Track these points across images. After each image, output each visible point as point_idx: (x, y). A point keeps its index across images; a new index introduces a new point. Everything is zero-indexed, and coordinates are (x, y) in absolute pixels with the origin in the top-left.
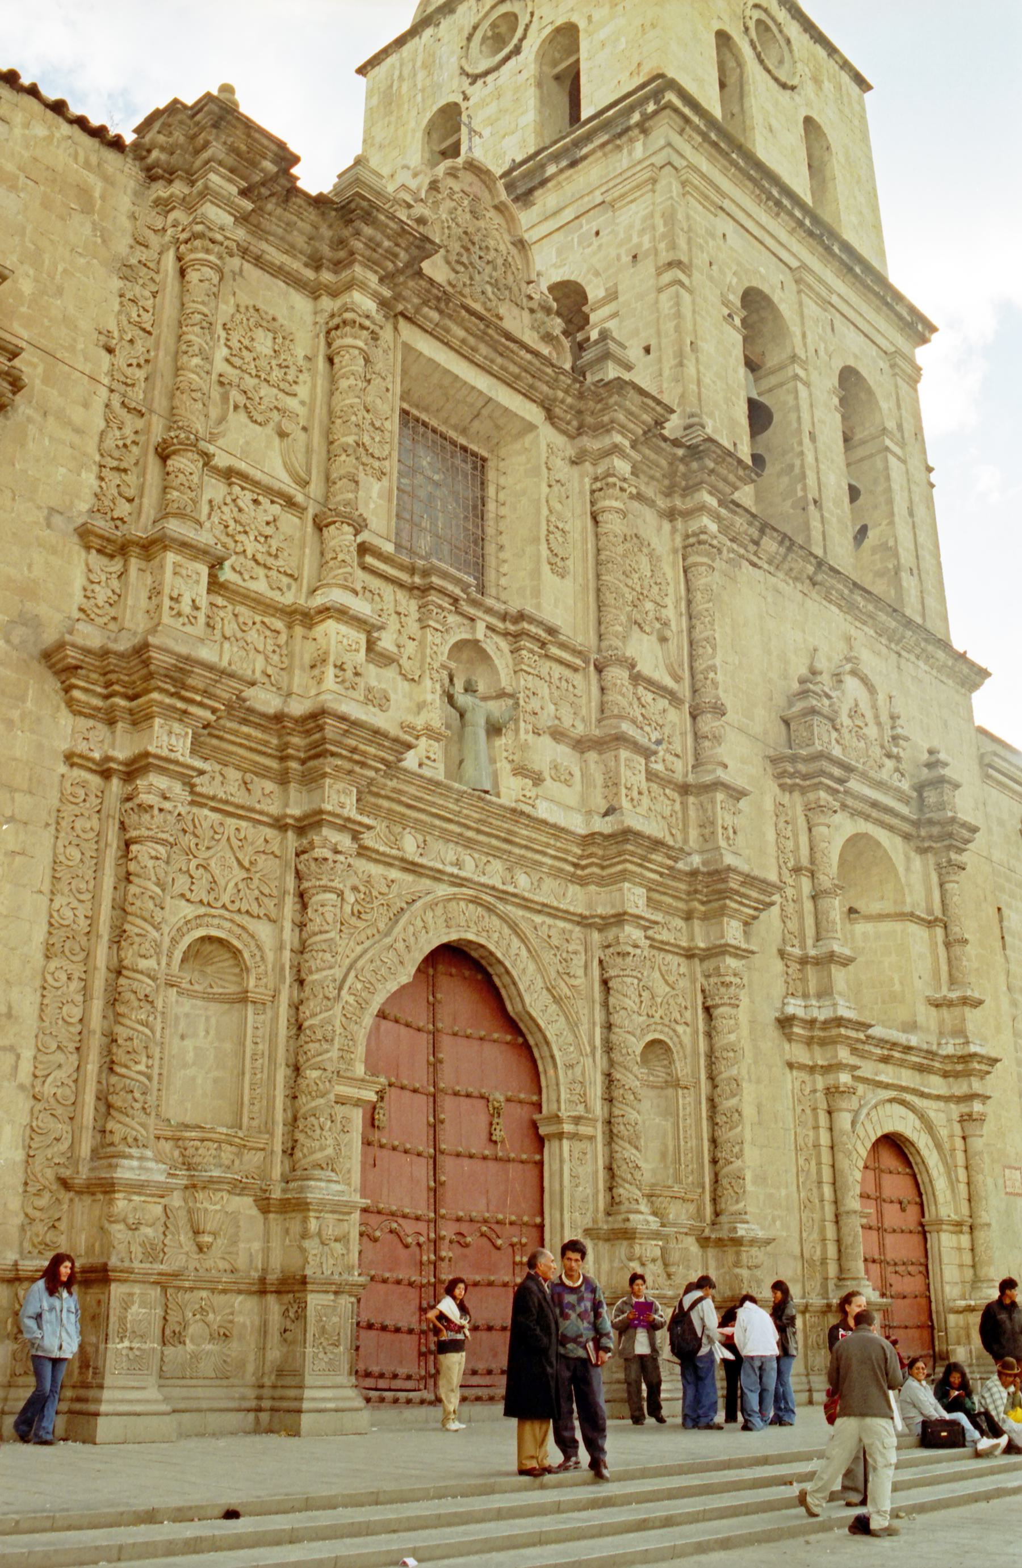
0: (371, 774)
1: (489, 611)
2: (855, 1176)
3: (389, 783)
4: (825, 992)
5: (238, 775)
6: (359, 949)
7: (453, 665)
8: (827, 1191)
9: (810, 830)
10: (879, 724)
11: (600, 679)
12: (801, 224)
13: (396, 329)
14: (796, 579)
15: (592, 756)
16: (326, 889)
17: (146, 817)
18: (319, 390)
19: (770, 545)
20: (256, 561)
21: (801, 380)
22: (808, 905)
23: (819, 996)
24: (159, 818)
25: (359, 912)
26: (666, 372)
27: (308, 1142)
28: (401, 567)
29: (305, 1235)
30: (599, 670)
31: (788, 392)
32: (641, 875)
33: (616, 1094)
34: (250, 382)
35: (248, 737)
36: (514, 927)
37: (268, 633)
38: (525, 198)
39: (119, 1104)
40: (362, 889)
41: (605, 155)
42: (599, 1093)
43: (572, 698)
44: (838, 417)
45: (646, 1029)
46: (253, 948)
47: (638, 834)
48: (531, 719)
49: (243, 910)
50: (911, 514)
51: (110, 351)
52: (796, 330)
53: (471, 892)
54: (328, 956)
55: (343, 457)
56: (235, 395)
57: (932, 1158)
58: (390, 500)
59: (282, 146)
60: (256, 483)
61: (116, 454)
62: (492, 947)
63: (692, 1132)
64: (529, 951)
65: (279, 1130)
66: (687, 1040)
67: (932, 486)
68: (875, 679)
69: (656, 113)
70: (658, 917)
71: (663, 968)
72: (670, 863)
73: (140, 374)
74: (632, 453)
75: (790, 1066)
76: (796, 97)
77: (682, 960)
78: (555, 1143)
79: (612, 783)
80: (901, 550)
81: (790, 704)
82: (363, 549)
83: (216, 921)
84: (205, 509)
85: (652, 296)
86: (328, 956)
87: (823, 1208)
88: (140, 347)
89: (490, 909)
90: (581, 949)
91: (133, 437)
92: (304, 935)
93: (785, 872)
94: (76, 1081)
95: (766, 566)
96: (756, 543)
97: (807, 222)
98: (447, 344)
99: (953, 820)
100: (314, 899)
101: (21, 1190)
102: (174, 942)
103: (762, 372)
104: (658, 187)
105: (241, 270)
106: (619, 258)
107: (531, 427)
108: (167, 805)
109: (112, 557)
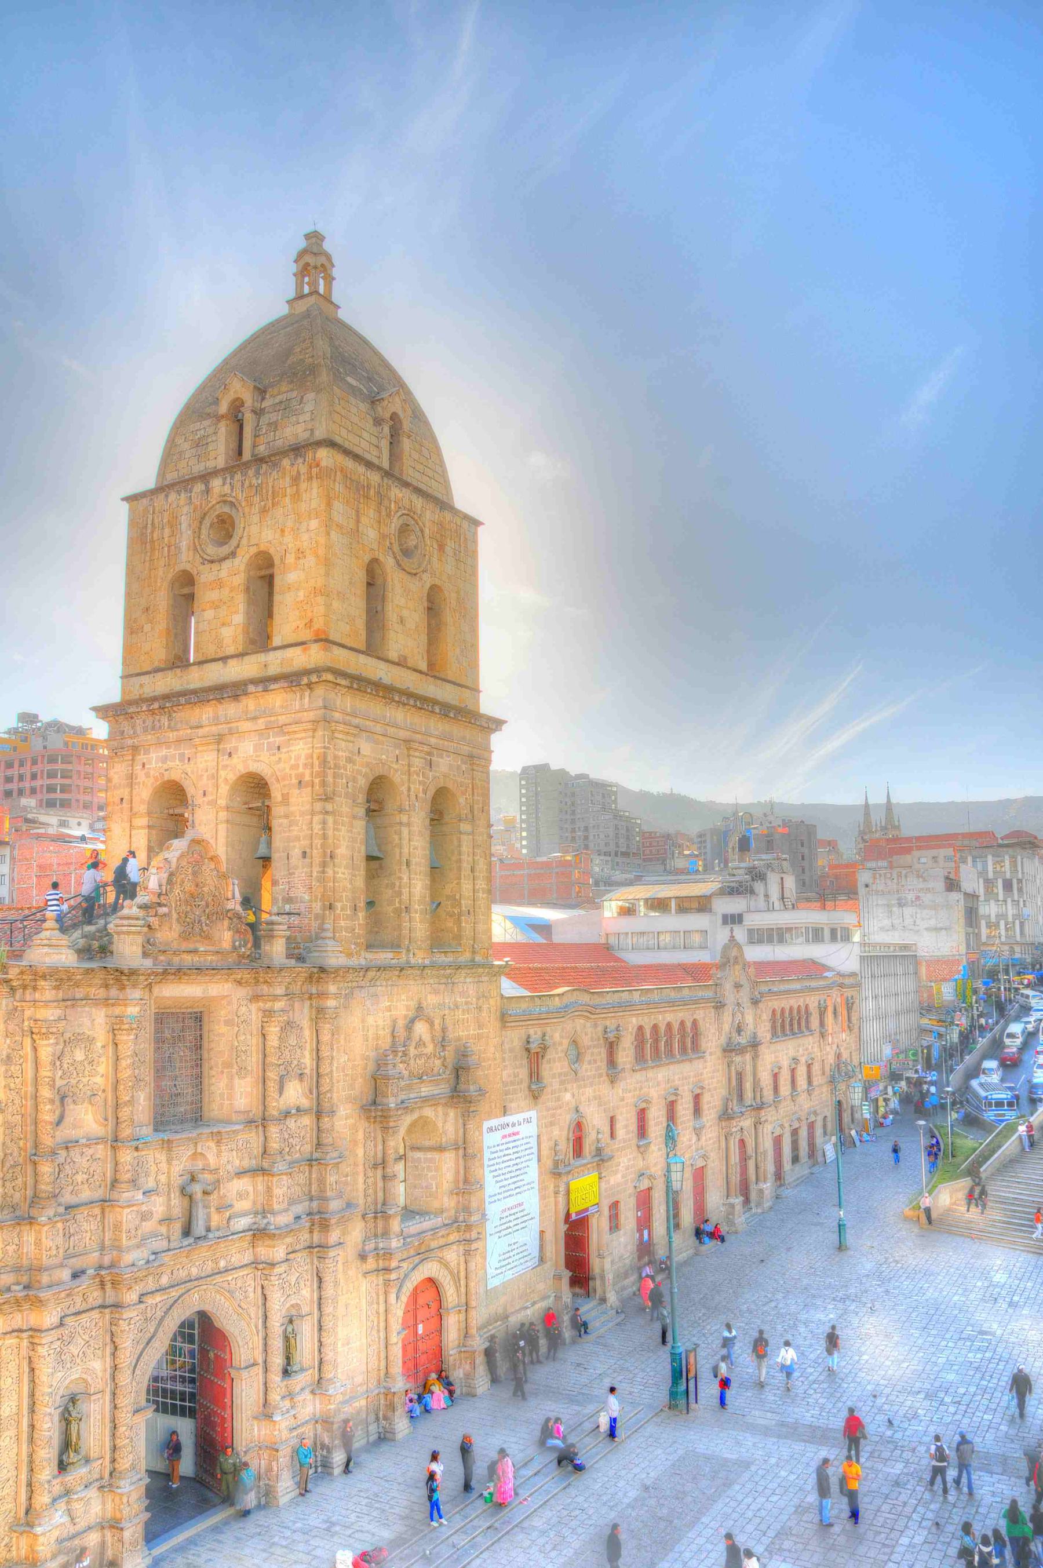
8: (382, 1335)
22: (380, 1184)
26: (315, 874)
50: (472, 870)
52: (404, 789)
76: (425, 576)
80: (463, 902)
104: (316, 734)
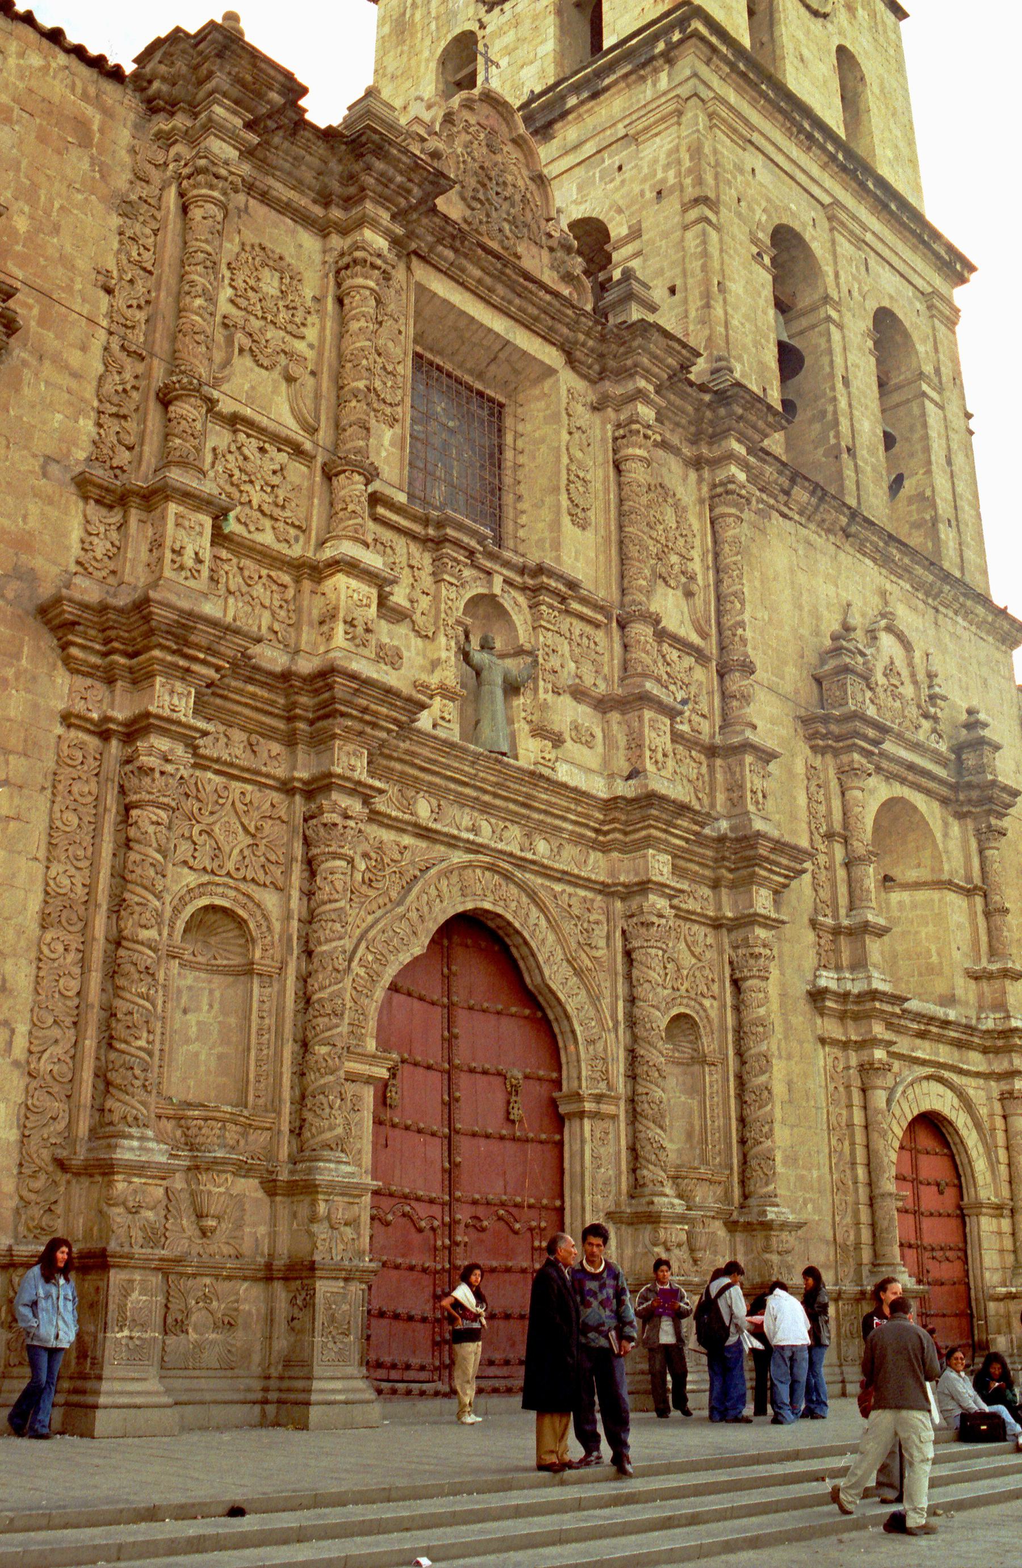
0: (383, 735)
1: (507, 564)
2: (890, 1156)
4: (860, 964)
5: (244, 736)
6: (370, 919)
7: (468, 621)
8: (861, 1172)
9: (843, 794)
10: (915, 683)
11: (623, 636)
12: (833, 158)
13: (409, 268)
14: (828, 531)
15: (615, 716)
16: (336, 856)
17: (147, 780)
18: (328, 332)
19: (801, 495)
20: (262, 512)
21: (834, 322)
22: (841, 873)
23: (853, 968)
24: (160, 781)
26: (693, 314)
27: (317, 1122)
28: (414, 518)
29: (313, 1219)
30: (622, 626)
31: (821, 334)
32: (666, 841)
33: (641, 1070)
34: (256, 324)
35: (253, 696)
36: (533, 896)
37: (275, 587)
38: (544, 131)
39: (119, 1081)
40: (373, 855)
41: (628, 86)
42: (622, 1070)
43: (594, 656)
44: (873, 360)
45: (671, 1002)
46: (259, 918)
47: (663, 798)
48: (551, 677)
49: (249, 877)
50: (949, 462)
51: (109, 291)
52: (828, 269)
53: (487, 859)
54: (337, 926)
55: (354, 403)
56: (240, 338)
57: (971, 1139)
58: (403, 449)
59: (289, 76)
60: (262, 430)
61: (116, 399)
62: (509, 917)
63: (719, 1111)
65: (287, 1108)
66: (713, 1014)
67: (971, 433)
68: (912, 636)
69: (681, 42)
70: (685, 886)
71: (689, 939)
72: (697, 828)
73: (141, 316)
74: (657, 399)
75: (823, 1041)
77: (708, 930)
78: (576, 1123)
79: (636, 744)
81: (823, 662)
82: (375, 499)
83: (220, 890)
84: (209, 458)
85: (679, 233)
86: (337, 926)
87: (856, 1190)
88: (140, 288)
89: (508, 877)
90: (603, 918)
91: (133, 382)
92: (313, 904)
93: (817, 837)
94: (73, 1057)
95: (797, 517)
96: (787, 493)
97: (840, 157)
98: (462, 284)
99: (994, 783)
100: (323, 866)
101: (15, 1172)
102: (176, 911)
103: (792, 314)
104: (684, 119)
105: (246, 207)
106: (642, 193)
107: (551, 372)
108: (169, 768)
109: (111, 507)
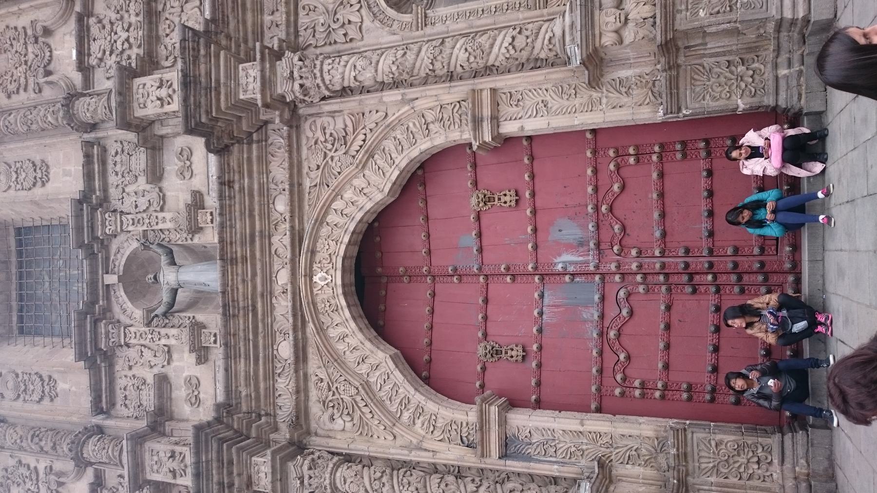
3: (244, 394)
25: (348, 414)
36: (320, 221)
64: (333, 201)
72: (202, 52)
89: (313, 252)
90: (319, 122)
